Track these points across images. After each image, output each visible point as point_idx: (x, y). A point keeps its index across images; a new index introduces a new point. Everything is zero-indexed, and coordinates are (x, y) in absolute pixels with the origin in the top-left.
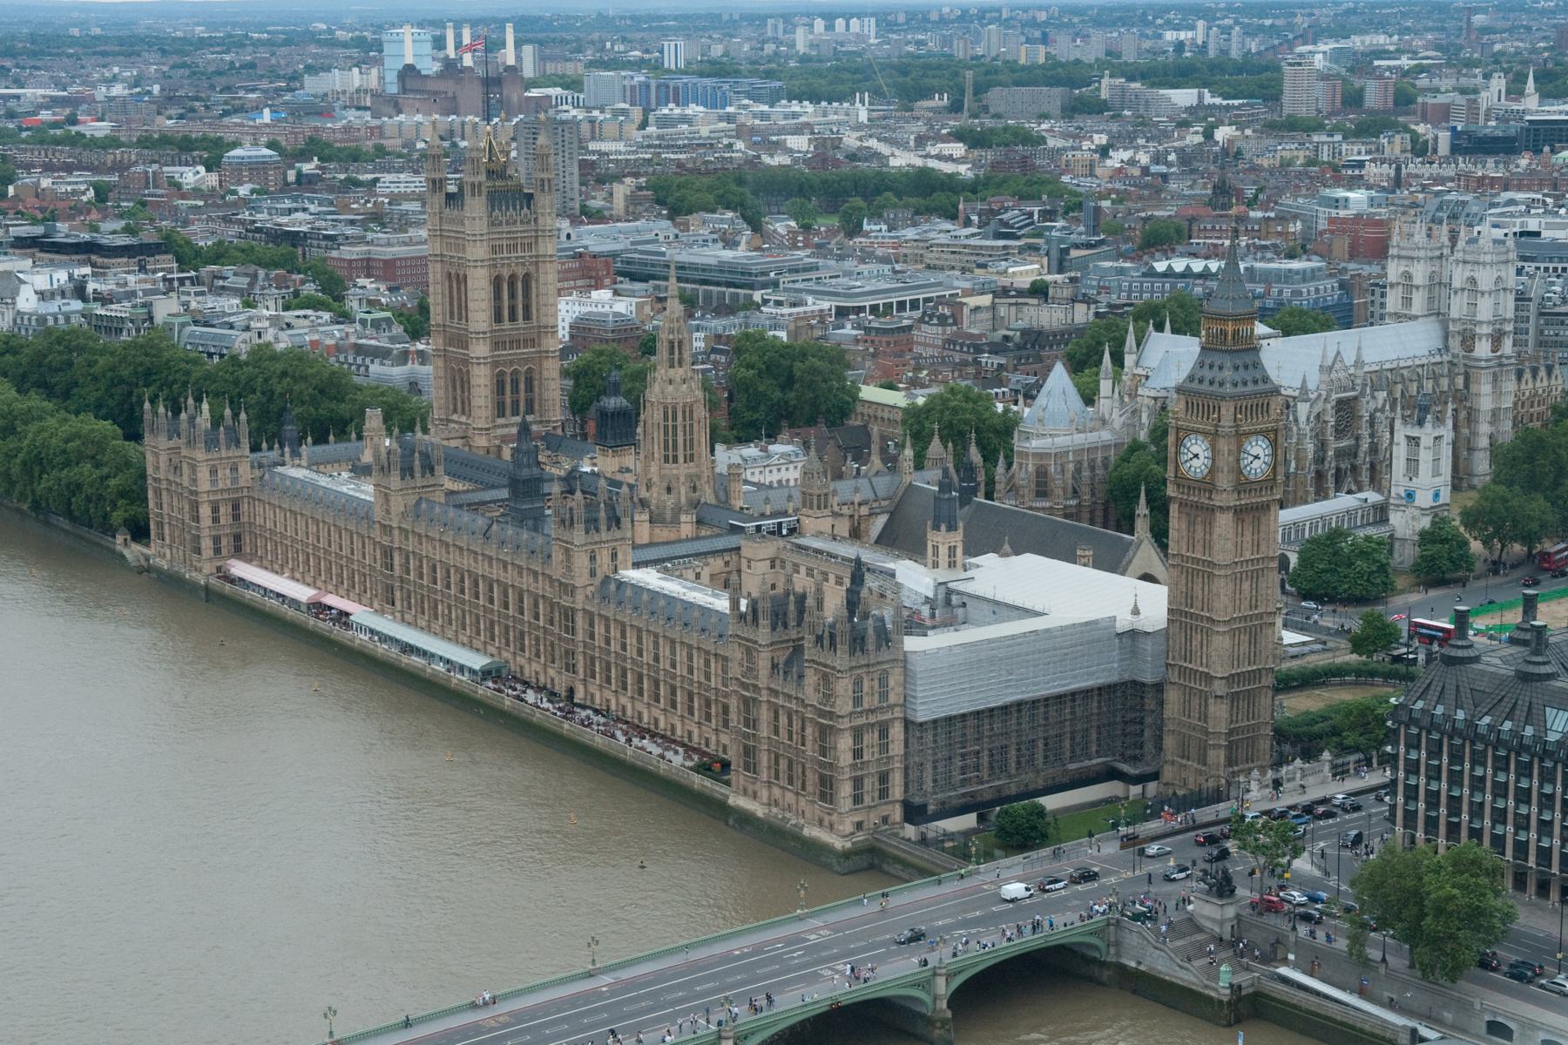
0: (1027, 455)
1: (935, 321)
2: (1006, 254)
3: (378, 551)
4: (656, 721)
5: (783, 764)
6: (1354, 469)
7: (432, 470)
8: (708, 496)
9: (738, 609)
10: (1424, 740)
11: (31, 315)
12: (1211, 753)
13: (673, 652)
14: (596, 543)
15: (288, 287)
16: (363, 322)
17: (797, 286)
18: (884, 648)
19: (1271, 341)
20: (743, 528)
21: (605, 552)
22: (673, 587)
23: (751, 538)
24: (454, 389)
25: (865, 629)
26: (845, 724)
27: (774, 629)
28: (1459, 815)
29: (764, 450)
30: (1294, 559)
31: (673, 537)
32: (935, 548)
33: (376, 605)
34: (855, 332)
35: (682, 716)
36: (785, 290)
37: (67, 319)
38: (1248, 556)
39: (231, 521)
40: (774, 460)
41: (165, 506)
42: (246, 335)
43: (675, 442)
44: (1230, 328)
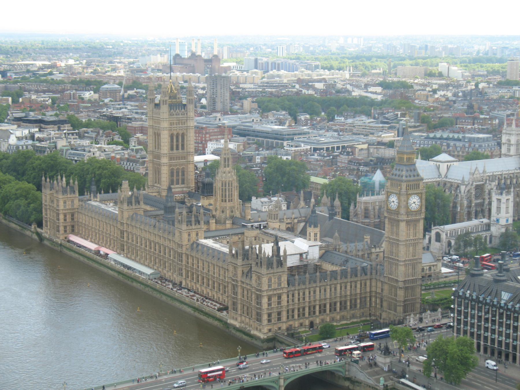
0: (361, 202)
1: (345, 154)
2: (382, 130)
4: (208, 293)
6: (483, 211)
7: (139, 203)
8: (237, 214)
9: (232, 252)
10: (463, 303)
11: (14, 145)
12: (398, 308)
13: (214, 269)
15: (110, 137)
16: (132, 150)
17: (300, 139)
18: (280, 267)
19: (455, 163)
21: (194, 233)
22: (217, 246)
23: (249, 229)
26: (265, 294)
27: (243, 260)
29: (270, 199)
32: (310, 233)
33: (118, 251)
36: (295, 141)
37: (27, 147)
38: (411, 238)
39: (70, 220)
41: (48, 215)
42: (89, 154)
44: (405, 156)
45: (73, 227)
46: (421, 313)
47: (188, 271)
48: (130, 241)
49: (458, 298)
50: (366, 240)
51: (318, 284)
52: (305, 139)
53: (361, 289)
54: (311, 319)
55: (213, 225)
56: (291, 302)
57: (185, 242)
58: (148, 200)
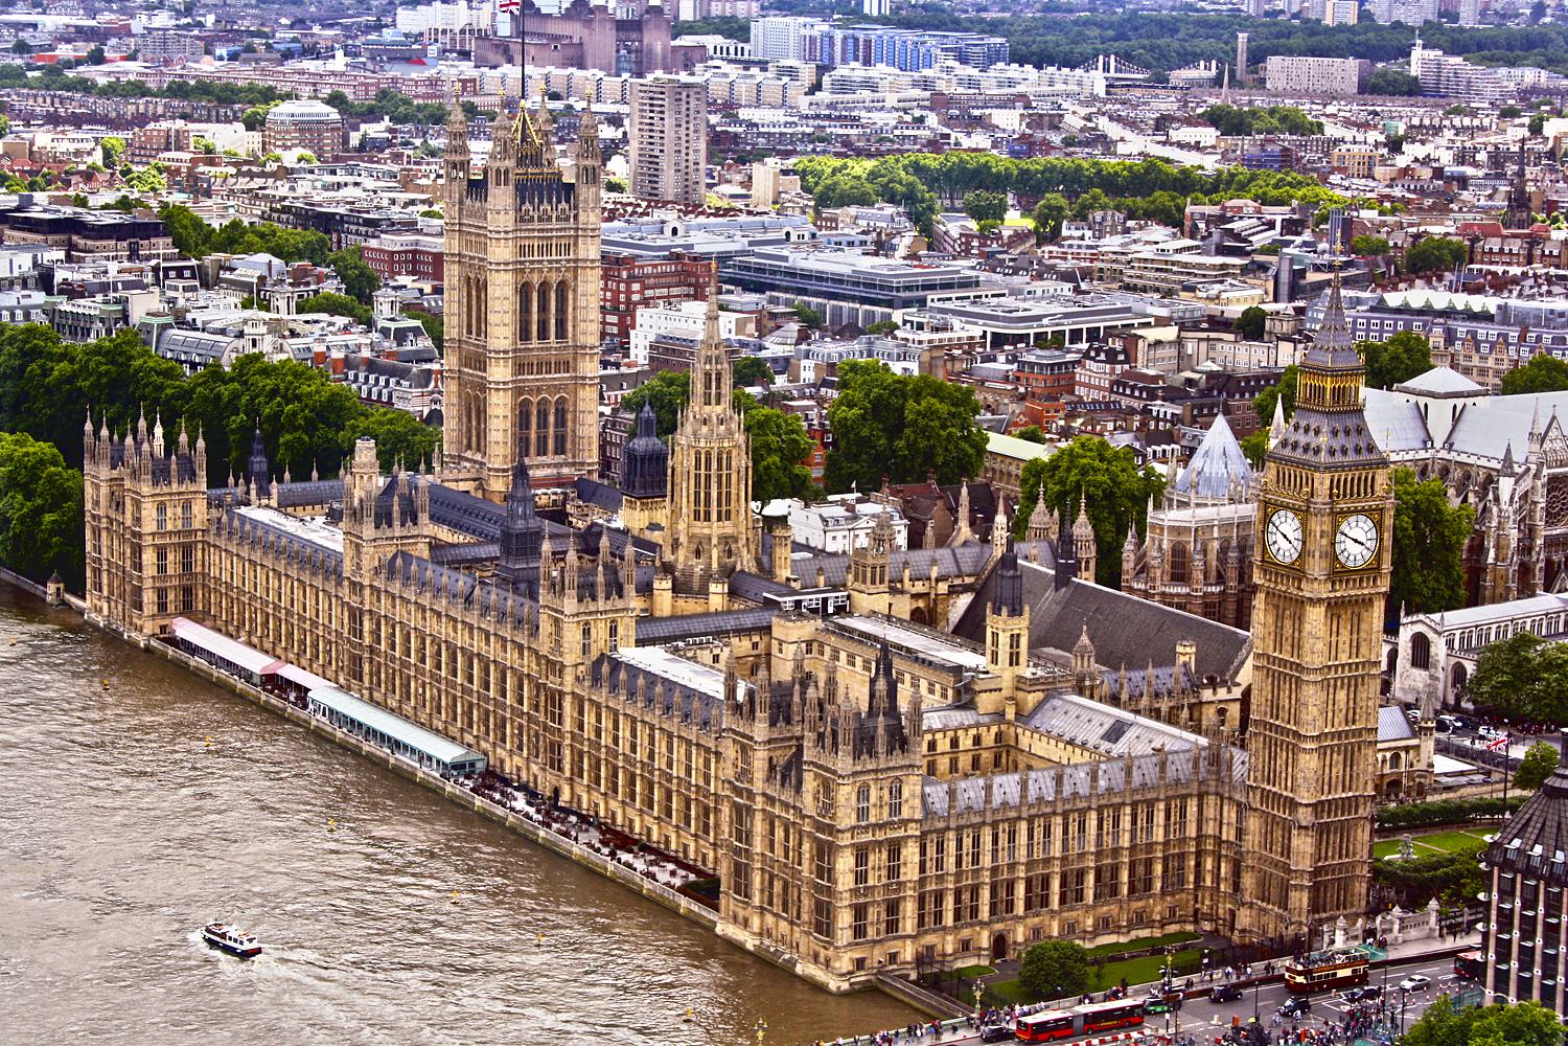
1: (1102, 357)
2: (1224, 271)
3: (346, 614)
8: (746, 561)
9: (735, 698)
10: (1518, 886)
12: (1294, 896)
13: (670, 750)
14: (591, 613)
15: (308, 284)
16: (385, 332)
18: (897, 752)
23: (785, 615)
25: (876, 728)
26: (845, 840)
27: (773, 724)
28: (1554, 977)
29: (850, 508)
30: (1470, 668)
31: (700, 609)
32: (995, 635)
33: (342, 680)
34: (1009, 367)
35: (677, 826)
37: (27, 316)
38: (1344, 659)
40: (862, 523)
42: (240, 343)
43: (708, 495)
45: (188, 591)
46: (1371, 914)
47: (581, 754)
49: (1501, 870)
50: (1182, 659)
52: (966, 303)
53: (1167, 827)
54: (999, 926)
55: (664, 599)
56: (931, 871)
57: (571, 656)
58: (448, 509)
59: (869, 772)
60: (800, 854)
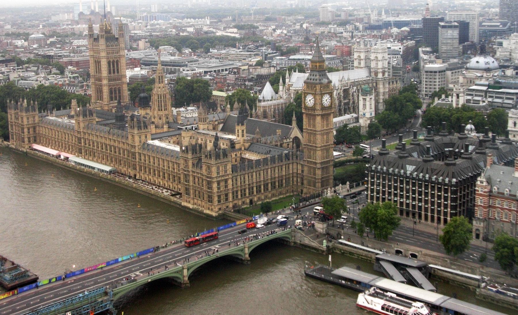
0: (261, 106)
1: (233, 73)
2: (250, 56)
5: (197, 192)
7: (92, 115)
8: (171, 120)
12: (317, 184)
15: (48, 70)
16: (70, 77)
18: (225, 158)
20: (182, 128)
24: (98, 93)
25: (220, 153)
26: (215, 180)
27: (193, 154)
31: (162, 132)
32: (238, 130)
33: (76, 154)
36: (189, 67)
38: (325, 128)
40: (189, 111)
42: (37, 82)
43: (161, 105)
44: (318, 65)
45: (35, 137)
48: (87, 146)
51: (255, 170)
53: (286, 171)
54: (251, 198)
56: (235, 186)
59: (219, 163)
60: (203, 184)
